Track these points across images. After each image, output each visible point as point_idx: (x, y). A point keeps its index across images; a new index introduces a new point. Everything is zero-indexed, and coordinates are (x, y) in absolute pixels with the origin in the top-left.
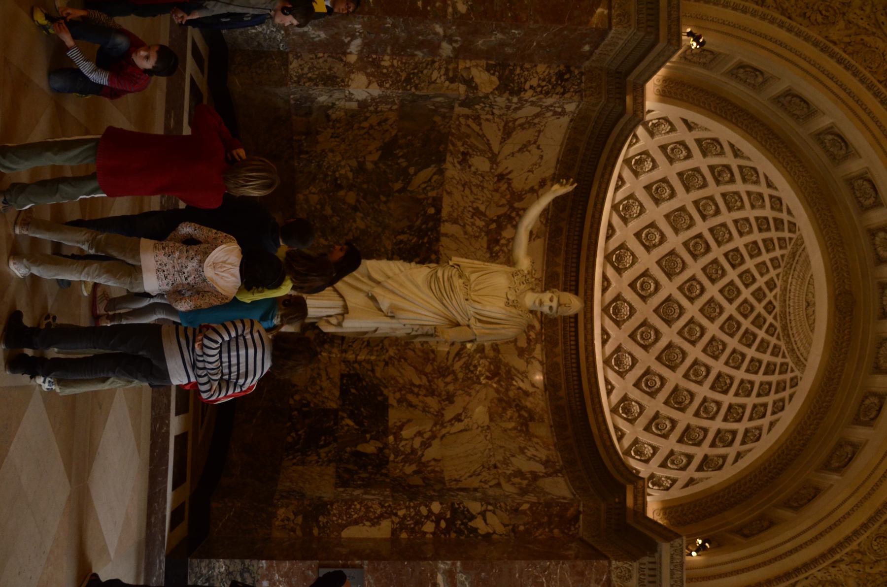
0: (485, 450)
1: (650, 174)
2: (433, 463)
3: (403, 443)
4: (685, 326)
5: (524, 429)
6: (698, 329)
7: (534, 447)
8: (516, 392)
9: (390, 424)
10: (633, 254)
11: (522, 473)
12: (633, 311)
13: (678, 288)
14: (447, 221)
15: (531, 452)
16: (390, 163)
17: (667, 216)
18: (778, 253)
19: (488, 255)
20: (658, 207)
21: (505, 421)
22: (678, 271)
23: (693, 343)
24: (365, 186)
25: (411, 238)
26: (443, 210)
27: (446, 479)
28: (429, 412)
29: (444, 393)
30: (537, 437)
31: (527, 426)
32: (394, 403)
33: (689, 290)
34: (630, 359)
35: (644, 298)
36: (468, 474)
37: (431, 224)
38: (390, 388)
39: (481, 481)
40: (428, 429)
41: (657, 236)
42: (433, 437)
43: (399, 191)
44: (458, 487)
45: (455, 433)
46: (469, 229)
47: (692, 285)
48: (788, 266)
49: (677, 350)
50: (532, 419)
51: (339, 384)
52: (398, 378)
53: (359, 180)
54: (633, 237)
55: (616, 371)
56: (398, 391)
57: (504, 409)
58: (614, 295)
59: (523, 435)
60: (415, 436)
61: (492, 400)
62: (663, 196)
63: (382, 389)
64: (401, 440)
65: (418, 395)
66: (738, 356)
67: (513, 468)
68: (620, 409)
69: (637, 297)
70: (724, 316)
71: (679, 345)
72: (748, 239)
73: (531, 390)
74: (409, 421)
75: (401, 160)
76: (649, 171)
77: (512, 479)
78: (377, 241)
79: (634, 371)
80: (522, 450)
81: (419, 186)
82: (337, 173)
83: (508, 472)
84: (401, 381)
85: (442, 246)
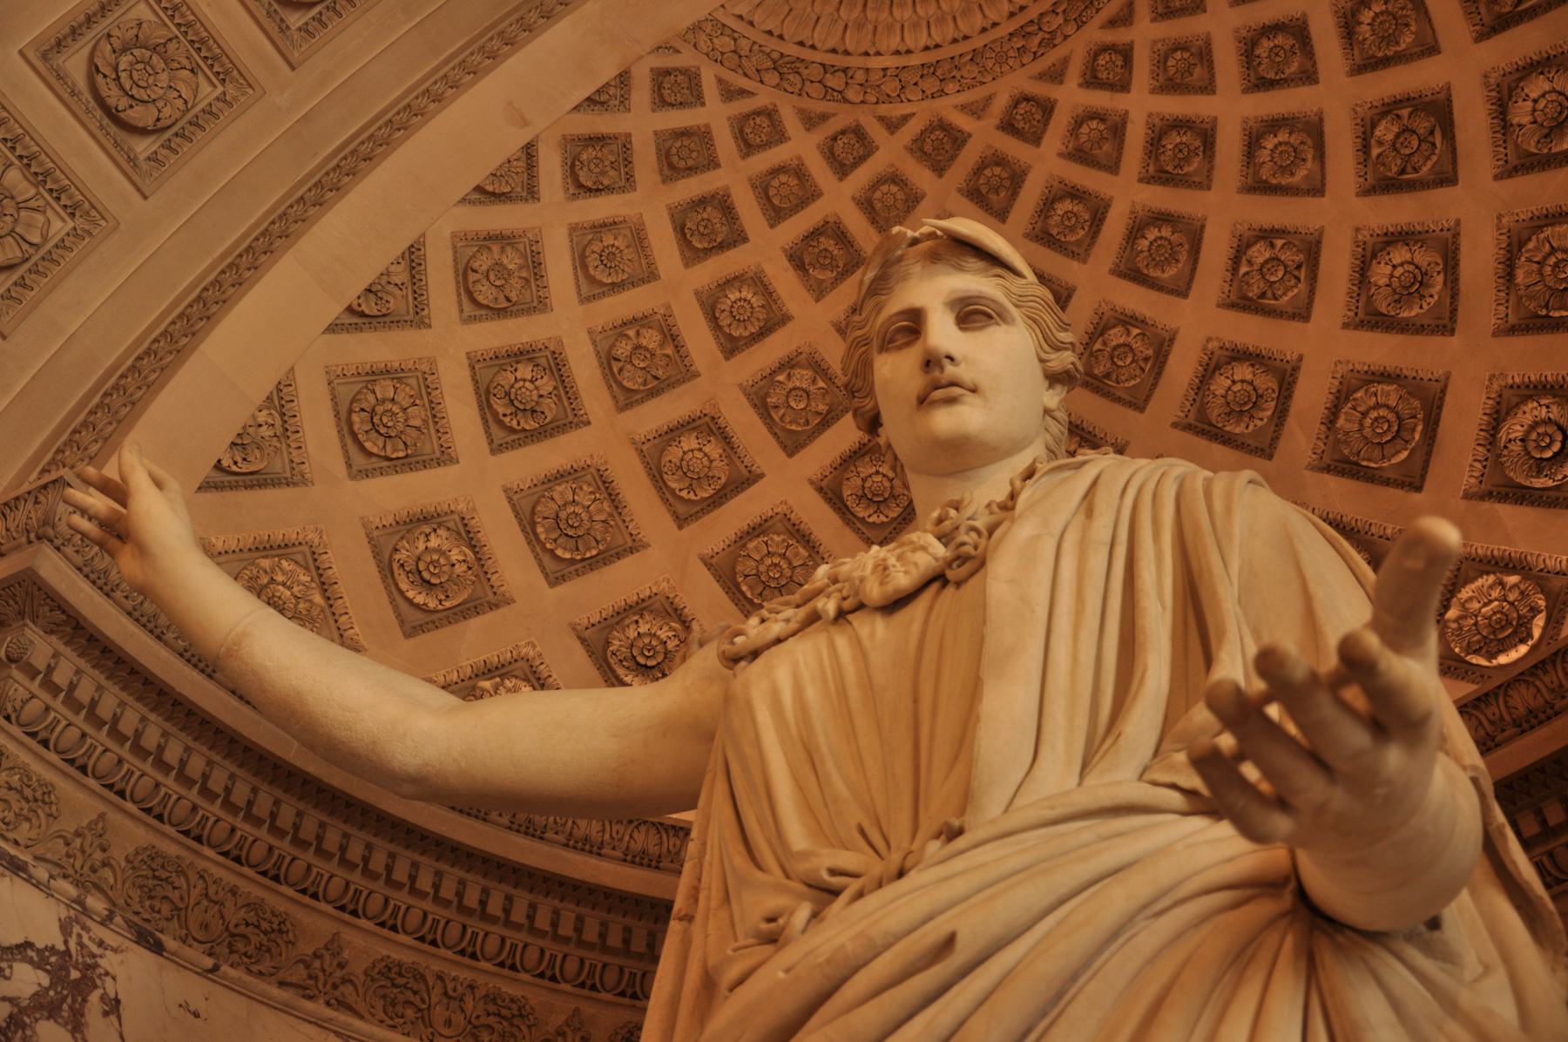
6: (1220, 384)
18: (802, 146)
23: (1287, 378)
34: (1465, 593)
48: (835, 81)
49: (1341, 422)
66: (1264, 155)
70: (1133, 299)
71: (1317, 427)
72: (785, 281)
79: (1518, 547)
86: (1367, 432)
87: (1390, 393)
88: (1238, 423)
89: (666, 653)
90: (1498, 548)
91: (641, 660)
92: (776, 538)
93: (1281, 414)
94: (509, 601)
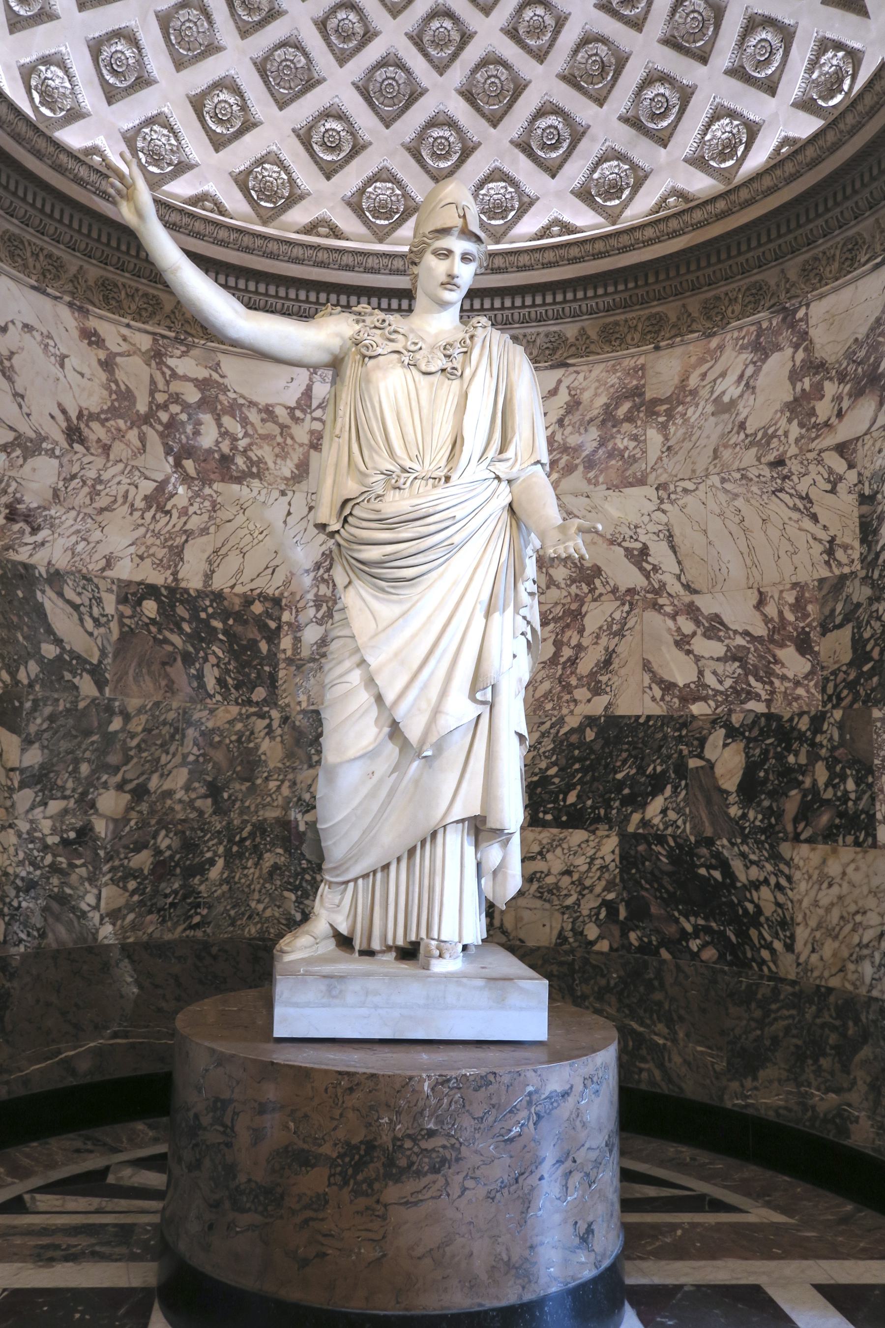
0: (726, 491)
1: (78, 79)
2: (771, 610)
3: (710, 680)
4: (426, 55)
5: (665, 407)
6: (435, 24)
7: (715, 381)
8: (569, 429)
9: (657, 710)
10: (260, 162)
11: (796, 400)
12: (384, 176)
13: (341, 67)
14: (175, 574)
15: (729, 388)
16: (28, 705)
17: (180, 64)
19: (256, 483)
20: (156, 82)
21: (644, 452)
22: (303, 60)
24: (85, 769)
25: (213, 660)
26: (148, 582)
27: (825, 573)
28: (624, 622)
29: (574, 589)
30: (684, 380)
31: (656, 402)
32: (603, 700)
33: (346, 39)
35: (357, 149)
36: (807, 523)
37: (181, 611)
38: (565, 711)
39: (833, 491)
40: (670, 623)
41: (222, 97)
42: (692, 611)
43: (100, 684)
44: (857, 544)
45: (679, 563)
46: (194, 523)
47: (337, 31)
49: (478, 75)
50: (637, 392)
51: (555, 831)
52: (537, 695)
53: (70, 784)
54: (221, 153)
55: (518, 218)
56: (570, 693)
57: (610, 455)
58: (349, 212)
59: (680, 408)
60: (689, 652)
61: (589, 481)
62: (131, 61)
63: (565, 729)
64: (701, 684)
65: (579, 647)
67: (783, 422)
68: (608, 204)
69: (354, 163)
73: (563, 397)
74: (647, 666)
75: (22, 676)
76: (70, 78)
77: (821, 419)
78: (217, 739)
79: (519, 177)
80: (723, 407)
81: (91, 634)
82: (52, 840)
83: (795, 430)
84: (546, 686)
85: (233, 587)
86: (486, 86)
87: (503, 74)
88: (435, 49)
89: (128, 65)
90: (513, 173)
91: (115, 67)
92: (195, 12)
93: (455, 56)
94: (58, 17)
